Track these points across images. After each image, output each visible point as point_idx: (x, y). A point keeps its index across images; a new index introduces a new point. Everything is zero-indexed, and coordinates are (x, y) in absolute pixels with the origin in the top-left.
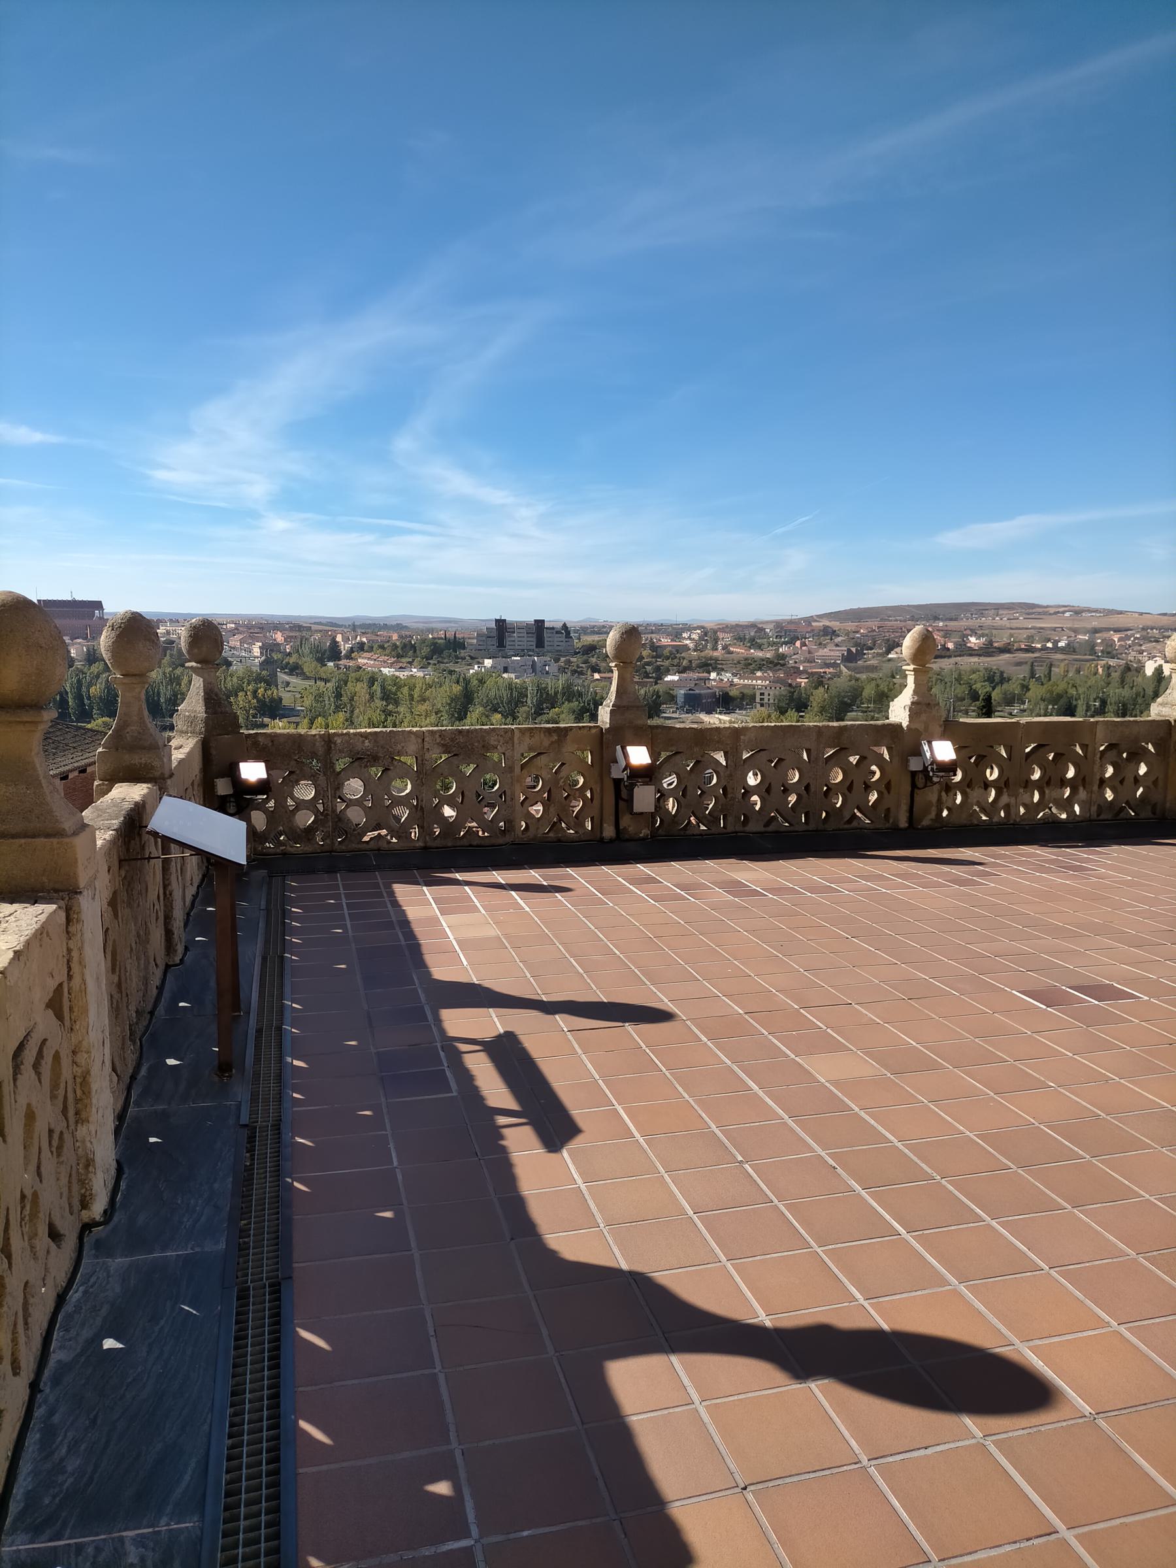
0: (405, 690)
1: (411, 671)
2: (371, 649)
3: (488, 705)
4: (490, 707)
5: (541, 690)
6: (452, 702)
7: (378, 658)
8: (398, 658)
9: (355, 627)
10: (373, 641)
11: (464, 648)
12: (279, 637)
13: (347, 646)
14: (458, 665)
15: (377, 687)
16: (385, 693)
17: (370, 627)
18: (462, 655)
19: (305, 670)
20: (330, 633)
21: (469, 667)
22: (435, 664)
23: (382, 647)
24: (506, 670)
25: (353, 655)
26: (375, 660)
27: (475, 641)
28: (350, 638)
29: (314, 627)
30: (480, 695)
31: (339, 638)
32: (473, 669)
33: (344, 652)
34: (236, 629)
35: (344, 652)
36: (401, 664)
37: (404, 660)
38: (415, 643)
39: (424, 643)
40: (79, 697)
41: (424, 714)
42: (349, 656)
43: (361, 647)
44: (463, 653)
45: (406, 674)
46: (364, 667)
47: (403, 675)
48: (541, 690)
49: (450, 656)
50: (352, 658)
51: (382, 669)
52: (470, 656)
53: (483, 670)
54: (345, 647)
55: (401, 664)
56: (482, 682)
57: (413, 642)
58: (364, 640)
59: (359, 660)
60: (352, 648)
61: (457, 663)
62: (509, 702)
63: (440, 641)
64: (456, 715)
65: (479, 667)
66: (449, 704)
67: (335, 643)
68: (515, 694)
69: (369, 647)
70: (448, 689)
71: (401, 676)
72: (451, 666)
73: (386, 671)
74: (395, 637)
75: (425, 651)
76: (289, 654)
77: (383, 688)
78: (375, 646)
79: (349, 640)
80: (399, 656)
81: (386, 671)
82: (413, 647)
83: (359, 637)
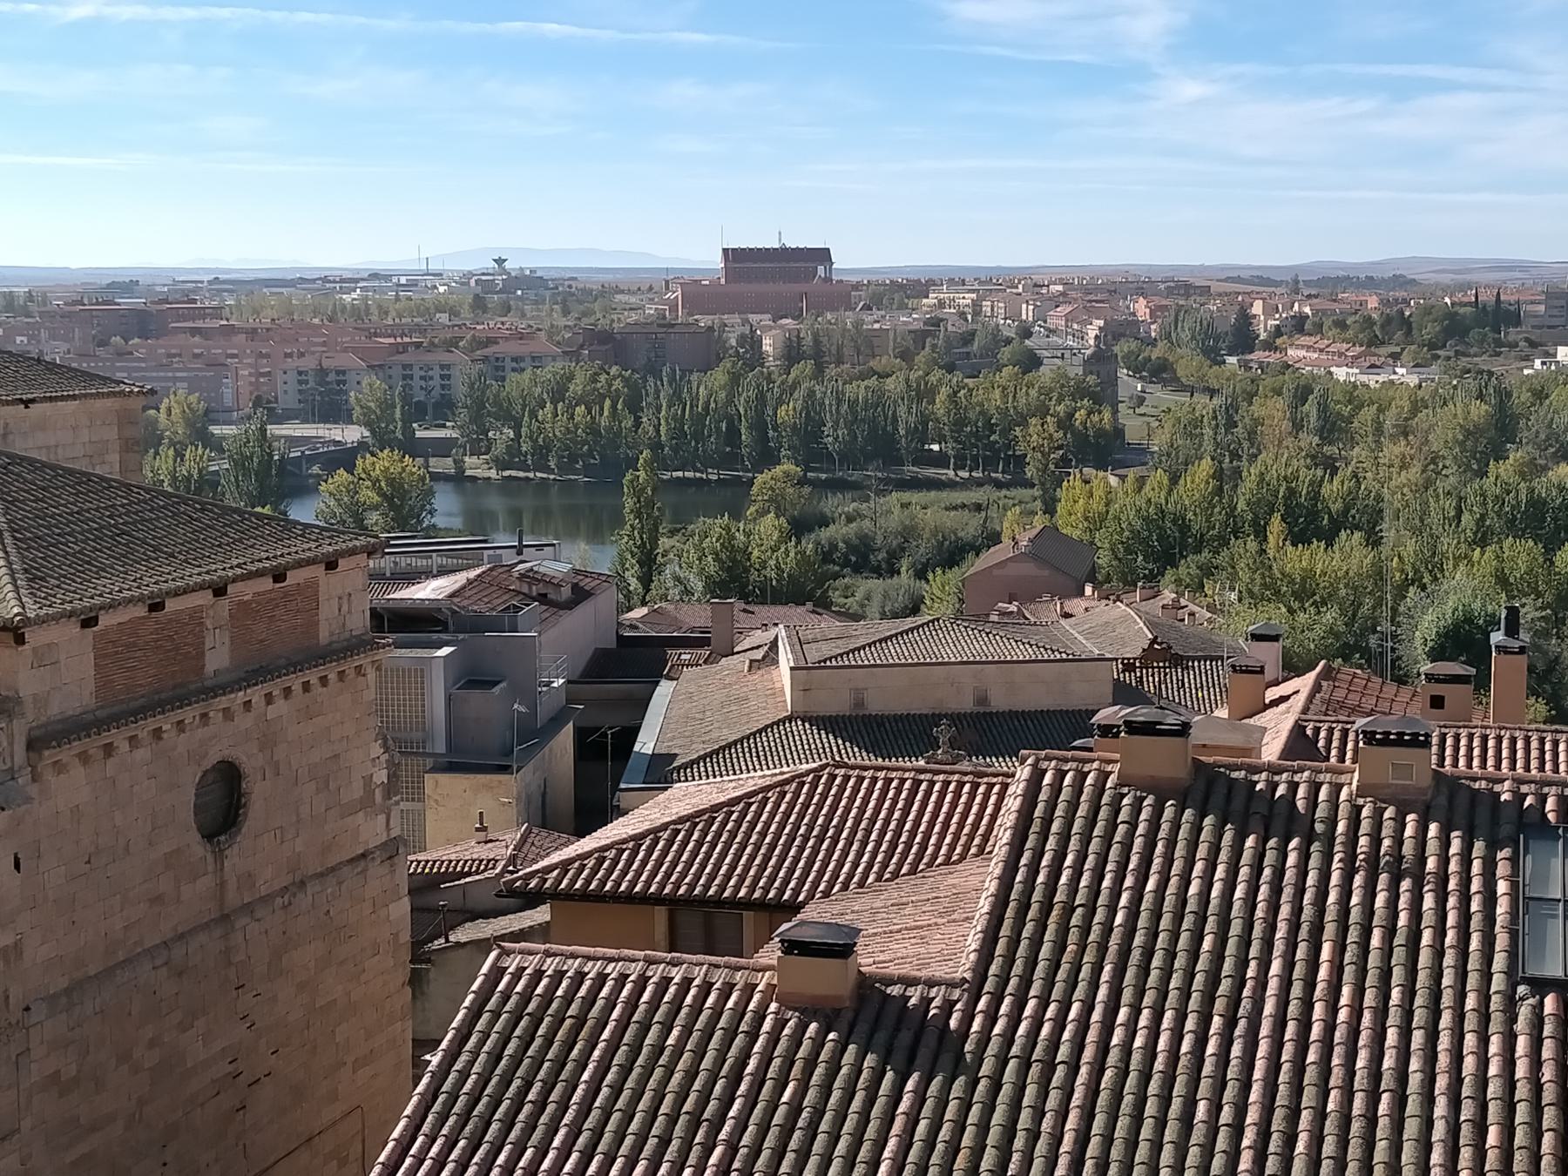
0: (1368, 413)
1: (1395, 373)
2: (1319, 329)
3: (1551, 445)
4: (1553, 450)
6: (1466, 438)
7: (1328, 346)
8: (1369, 346)
9: (1295, 284)
10: (1324, 312)
11: (1518, 323)
12: (1141, 308)
13: (1271, 322)
14: (1501, 359)
15: (1310, 408)
16: (1326, 420)
17: (1331, 283)
18: (1511, 338)
19: (1180, 373)
20: (1240, 298)
21: (1524, 364)
22: (1449, 358)
23: (1341, 325)
25: (1279, 341)
26: (1321, 351)
27: (1542, 308)
28: (1280, 307)
29: (1216, 287)
30: (1533, 426)
31: (1257, 308)
32: (1532, 367)
33: (1263, 336)
34: (1063, 294)
35: (1263, 336)
36: (1374, 360)
37: (1384, 350)
38: (1410, 316)
39: (1430, 313)
40: (759, 426)
41: (1397, 462)
42: (1269, 346)
43: (1299, 325)
44: (1513, 334)
45: (1381, 378)
46: (1297, 365)
47: (1373, 380)
49: (1482, 341)
50: (1276, 349)
51: (1332, 369)
52: (1527, 340)
53: (1553, 368)
55: (1374, 360)
56: (1540, 395)
57: (1407, 313)
58: (1307, 310)
59: (1290, 352)
60: (1277, 327)
61: (1498, 354)
63: (1462, 310)
64: (1475, 467)
65: (1543, 363)
66: (1462, 444)
67: (1245, 319)
69: (1314, 324)
70: (1459, 411)
71: (1372, 384)
72: (1483, 362)
73: (1341, 373)
74: (1373, 302)
75: (1430, 330)
76: (1154, 343)
77: (1323, 408)
78: (1327, 323)
79: (1277, 312)
80: (1374, 342)
81: (1341, 373)
82: (1406, 324)
83: (1296, 305)
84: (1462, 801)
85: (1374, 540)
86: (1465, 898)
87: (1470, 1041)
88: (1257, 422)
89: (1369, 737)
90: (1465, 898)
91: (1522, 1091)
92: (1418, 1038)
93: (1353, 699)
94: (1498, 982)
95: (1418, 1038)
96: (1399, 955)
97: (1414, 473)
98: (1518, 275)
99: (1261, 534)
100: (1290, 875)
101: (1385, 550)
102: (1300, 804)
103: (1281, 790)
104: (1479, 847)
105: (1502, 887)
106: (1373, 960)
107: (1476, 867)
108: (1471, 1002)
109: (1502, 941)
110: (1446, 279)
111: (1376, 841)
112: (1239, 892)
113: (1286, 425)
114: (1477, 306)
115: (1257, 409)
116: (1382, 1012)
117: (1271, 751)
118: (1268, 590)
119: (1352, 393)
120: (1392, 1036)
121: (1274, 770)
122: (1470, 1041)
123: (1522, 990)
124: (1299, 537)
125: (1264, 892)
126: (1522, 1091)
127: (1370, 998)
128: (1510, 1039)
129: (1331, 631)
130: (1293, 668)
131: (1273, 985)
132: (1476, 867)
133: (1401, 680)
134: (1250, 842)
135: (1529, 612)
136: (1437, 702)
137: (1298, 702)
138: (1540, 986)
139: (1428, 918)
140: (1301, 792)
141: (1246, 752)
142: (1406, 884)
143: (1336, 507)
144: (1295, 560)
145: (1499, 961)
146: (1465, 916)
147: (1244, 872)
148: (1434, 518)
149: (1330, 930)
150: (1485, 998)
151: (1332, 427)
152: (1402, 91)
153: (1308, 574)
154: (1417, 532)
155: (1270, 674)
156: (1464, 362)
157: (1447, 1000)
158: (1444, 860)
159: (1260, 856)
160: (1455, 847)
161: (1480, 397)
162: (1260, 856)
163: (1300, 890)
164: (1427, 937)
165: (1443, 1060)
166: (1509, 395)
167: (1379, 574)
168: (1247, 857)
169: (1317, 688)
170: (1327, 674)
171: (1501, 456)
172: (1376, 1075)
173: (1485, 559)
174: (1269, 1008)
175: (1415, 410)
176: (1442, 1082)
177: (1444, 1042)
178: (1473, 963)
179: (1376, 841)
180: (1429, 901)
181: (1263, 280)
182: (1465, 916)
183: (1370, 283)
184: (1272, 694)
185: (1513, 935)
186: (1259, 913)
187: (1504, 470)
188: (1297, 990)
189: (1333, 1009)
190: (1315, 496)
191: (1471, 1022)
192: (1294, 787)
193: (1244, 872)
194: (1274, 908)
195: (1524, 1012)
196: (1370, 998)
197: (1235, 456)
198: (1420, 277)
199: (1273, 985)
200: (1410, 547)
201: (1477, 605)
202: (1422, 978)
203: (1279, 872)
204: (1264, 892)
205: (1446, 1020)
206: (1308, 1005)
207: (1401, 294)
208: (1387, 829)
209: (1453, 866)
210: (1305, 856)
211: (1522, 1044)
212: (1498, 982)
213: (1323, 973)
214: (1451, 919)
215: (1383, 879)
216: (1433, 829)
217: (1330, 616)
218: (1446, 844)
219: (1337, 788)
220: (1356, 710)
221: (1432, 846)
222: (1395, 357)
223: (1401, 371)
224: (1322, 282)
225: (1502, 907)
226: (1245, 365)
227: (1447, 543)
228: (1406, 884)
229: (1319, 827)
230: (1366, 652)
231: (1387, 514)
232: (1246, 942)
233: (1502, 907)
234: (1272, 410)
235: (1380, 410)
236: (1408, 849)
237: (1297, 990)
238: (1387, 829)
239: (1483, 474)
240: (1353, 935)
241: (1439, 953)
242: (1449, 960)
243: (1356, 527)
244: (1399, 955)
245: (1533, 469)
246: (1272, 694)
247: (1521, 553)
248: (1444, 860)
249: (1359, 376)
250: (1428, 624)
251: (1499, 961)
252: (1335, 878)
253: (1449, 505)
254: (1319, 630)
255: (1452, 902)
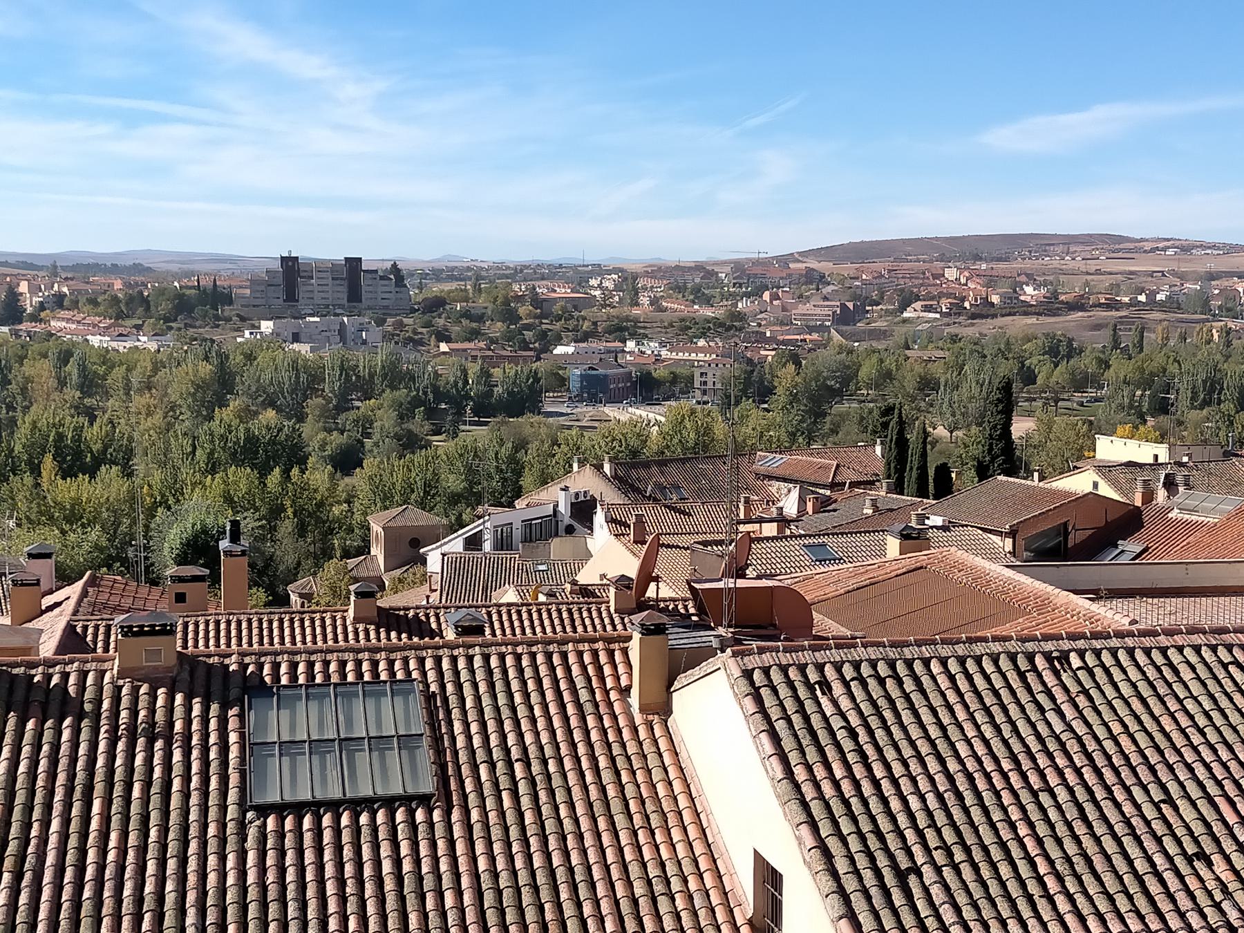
0: (119, 372)
1: (139, 340)
2: (75, 305)
3: (260, 396)
4: (262, 399)
5: (346, 369)
6: (196, 390)
7: (84, 319)
8: (117, 319)
9: (54, 268)
10: (79, 291)
11: (231, 302)
13: (35, 299)
14: (219, 330)
15: (72, 368)
16: (85, 377)
17: (83, 269)
18: (226, 314)
20: (8, 279)
21: (236, 334)
22: (179, 329)
23: (93, 302)
24: (296, 338)
25: (43, 315)
26: (79, 322)
27: (248, 291)
28: (43, 287)
30: (244, 383)
31: (23, 287)
32: (243, 337)
33: (29, 310)
35: (29, 310)
36: (121, 330)
38: (148, 296)
39: (163, 294)
41: (144, 411)
42: (34, 318)
43: (59, 301)
44: (228, 310)
45: (128, 345)
46: (59, 334)
47: (122, 346)
48: (346, 369)
49: (205, 317)
50: (41, 321)
51: (88, 337)
52: (238, 315)
53: (258, 337)
54: (29, 303)
55: (121, 330)
56: (250, 357)
57: (146, 294)
58: (65, 290)
59: (52, 323)
60: (41, 303)
61: (218, 326)
62: (293, 391)
63: (188, 292)
64: (205, 413)
65: (251, 333)
66: (194, 395)
67: (14, 296)
68: (303, 377)
69: (72, 301)
70: (190, 371)
71: (121, 349)
72: (206, 332)
73: (95, 340)
74: (118, 285)
75: (164, 307)
77: (83, 368)
78: (82, 300)
79: (41, 291)
80: (120, 316)
81: (95, 340)
82: (145, 302)
83: (56, 285)
84: (201, 672)
85: (128, 473)
86: (205, 749)
87: (212, 861)
88: (28, 380)
89: (127, 631)
90: (205, 749)
91: (252, 893)
92: (172, 864)
93: (114, 600)
94: (232, 812)
95: (172, 864)
96: (155, 801)
97: (157, 419)
98: (231, 266)
99: (36, 470)
100: (65, 749)
101: (138, 481)
102: (72, 690)
103: (55, 680)
104: (214, 708)
105: (233, 737)
106: (135, 808)
107: (213, 724)
108: (212, 830)
109: (234, 779)
110: (174, 268)
111: (134, 713)
112: (22, 768)
113: (53, 383)
114: (199, 289)
115: (28, 369)
116: (143, 849)
117: (47, 648)
118: (45, 515)
119: (105, 356)
120: (151, 867)
121: (49, 663)
122: (212, 861)
123: (250, 815)
124: (67, 473)
125: (43, 764)
126: (252, 893)
127: (133, 839)
128: (242, 855)
129: (97, 547)
130: (65, 577)
131: (53, 840)
132: (213, 724)
133: (154, 582)
134: (30, 725)
135: (249, 522)
136: (180, 598)
137: (69, 606)
138: (263, 811)
139: (177, 769)
140: (72, 680)
141: (26, 651)
142: (159, 744)
143: (97, 447)
144: (66, 491)
145: (233, 796)
146: (206, 763)
147: (26, 750)
148: (175, 454)
149: (99, 788)
150: (223, 826)
151: (90, 383)
152: (132, 120)
153: (76, 502)
154: (162, 465)
155: (44, 586)
156: (191, 332)
157: (193, 831)
158: (188, 722)
159: (39, 734)
160: (196, 710)
161: (206, 358)
162: (39, 734)
163: (73, 760)
164: (176, 784)
165: (192, 879)
166: (227, 357)
167: (132, 498)
168: (28, 737)
169: (84, 593)
170: (92, 582)
171: (223, 404)
172: (139, 900)
173: (215, 483)
174: (50, 859)
175: (155, 370)
176: (191, 897)
177: (192, 865)
178: (213, 800)
179: (134, 713)
180: (177, 756)
181: (27, 265)
182: (206, 763)
183: (115, 269)
184: (47, 601)
185: (243, 774)
186: (40, 782)
187: (226, 414)
188: (73, 842)
189: (103, 852)
190: (78, 439)
191: (212, 846)
192: (65, 676)
193: (26, 750)
194: (52, 775)
195: (252, 832)
196: (133, 839)
197: (11, 407)
198: (159, 265)
199: (53, 840)
200: (157, 476)
201: (210, 521)
202: (174, 817)
203: (56, 747)
204: (43, 764)
205: (193, 846)
206: (82, 852)
207: (140, 279)
208: (143, 702)
209: (195, 726)
210: (76, 731)
211: (251, 857)
212: (232, 812)
213: (94, 824)
214: (195, 767)
215: (141, 742)
216: (179, 698)
217: (95, 534)
218: (188, 709)
219: (102, 674)
220: (117, 609)
221: (179, 712)
222: (138, 328)
223: (144, 339)
224: (76, 267)
225: (234, 752)
226: (16, 334)
227: (186, 473)
228: (159, 744)
229: (88, 707)
230: (125, 561)
231: (138, 451)
232: (28, 808)
233: (234, 752)
234: (40, 371)
235: (129, 370)
236: (160, 716)
237: (73, 842)
238: (143, 702)
239: (210, 418)
240: (118, 790)
241: (186, 795)
242: (194, 800)
243: (113, 462)
244: (155, 801)
245: (247, 414)
246: (47, 601)
247: (241, 478)
248: (188, 722)
249: (110, 343)
250: (173, 536)
251: (233, 796)
252: (102, 746)
253: (187, 444)
254: (86, 547)
255: (195, 753)
